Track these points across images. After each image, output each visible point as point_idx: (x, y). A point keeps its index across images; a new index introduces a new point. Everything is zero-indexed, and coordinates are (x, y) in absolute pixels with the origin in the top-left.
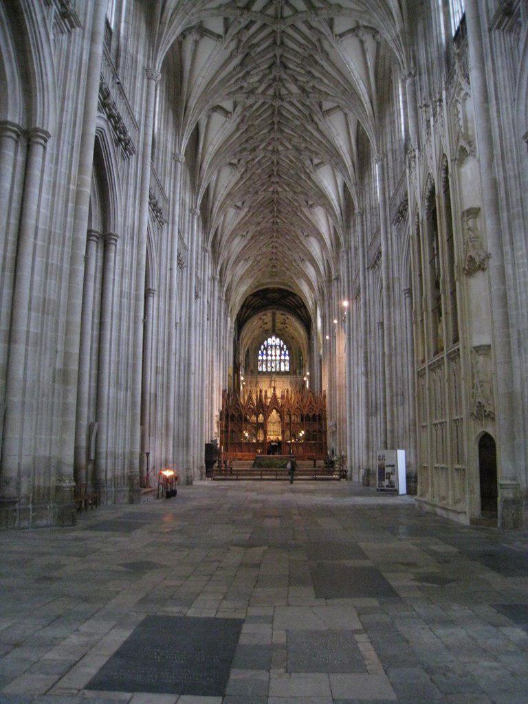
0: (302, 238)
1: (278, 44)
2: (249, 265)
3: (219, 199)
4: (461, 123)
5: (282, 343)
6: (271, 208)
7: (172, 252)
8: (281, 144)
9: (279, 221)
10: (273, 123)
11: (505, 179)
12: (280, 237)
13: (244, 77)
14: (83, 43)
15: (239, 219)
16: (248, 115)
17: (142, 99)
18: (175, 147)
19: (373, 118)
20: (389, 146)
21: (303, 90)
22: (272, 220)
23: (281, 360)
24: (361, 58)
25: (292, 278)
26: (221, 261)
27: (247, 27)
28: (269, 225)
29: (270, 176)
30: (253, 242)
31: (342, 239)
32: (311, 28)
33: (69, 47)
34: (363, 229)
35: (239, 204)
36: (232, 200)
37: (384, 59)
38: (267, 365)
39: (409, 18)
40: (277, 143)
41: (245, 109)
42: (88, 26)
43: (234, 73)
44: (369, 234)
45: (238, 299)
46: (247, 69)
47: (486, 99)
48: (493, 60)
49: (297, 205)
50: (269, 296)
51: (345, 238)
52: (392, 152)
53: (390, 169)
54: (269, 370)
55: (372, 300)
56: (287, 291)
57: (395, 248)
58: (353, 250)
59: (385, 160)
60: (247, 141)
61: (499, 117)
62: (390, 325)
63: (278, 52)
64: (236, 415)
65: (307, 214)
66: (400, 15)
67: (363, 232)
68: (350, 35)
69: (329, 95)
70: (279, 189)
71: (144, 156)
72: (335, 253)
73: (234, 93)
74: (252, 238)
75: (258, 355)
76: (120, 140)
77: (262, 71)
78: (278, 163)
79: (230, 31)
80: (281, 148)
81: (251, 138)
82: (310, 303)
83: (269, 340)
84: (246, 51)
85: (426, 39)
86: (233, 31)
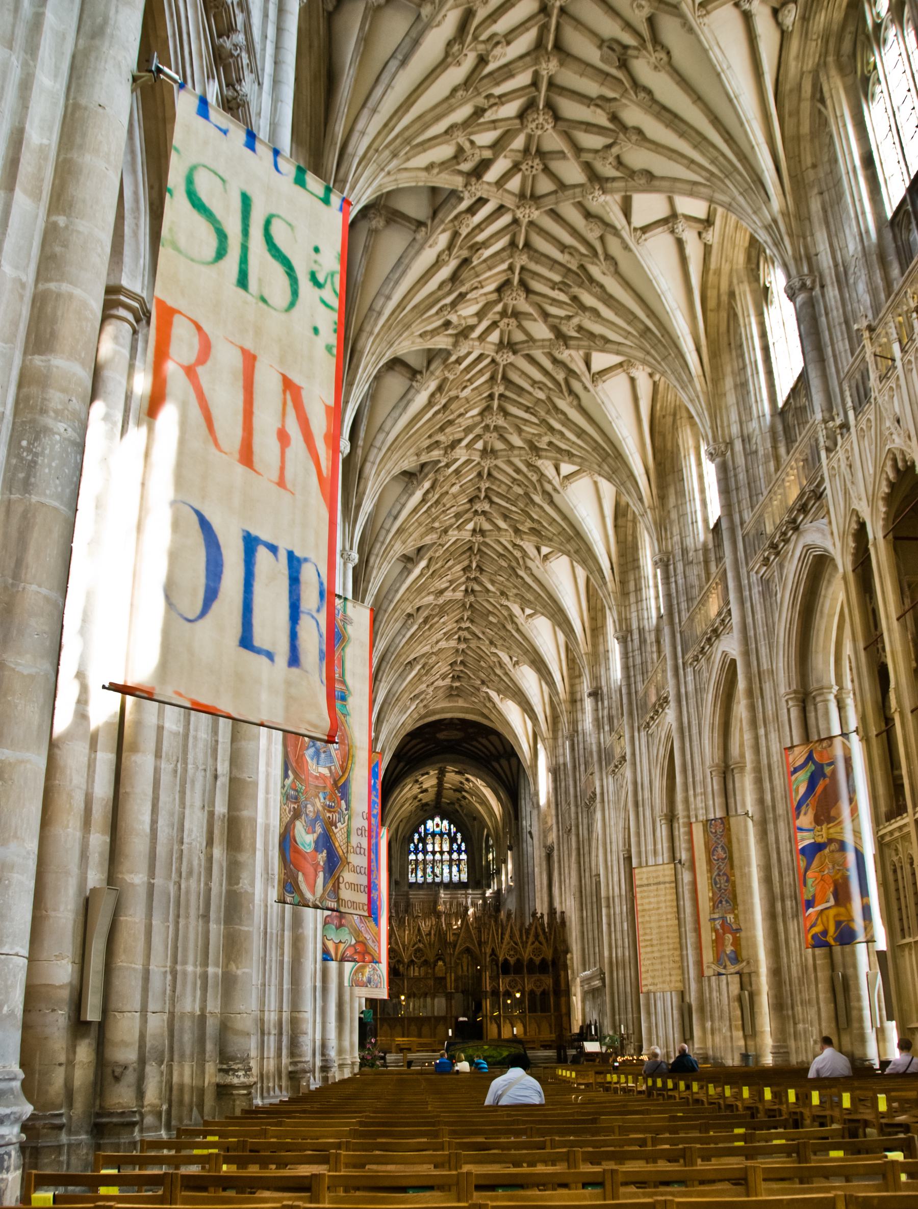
0: (520, 618)
1: (521, 246)
3: (381, 539)
5: (453, 829)
6: (466, 563)
8: (502, 438)
9: (477, 588)
10: (491, 396)
12: (476, 620)
13: (454, 304)
16: (451, 377)
19: (702, 378)
21: (560, 335)
22: (463, 588)
23: (451, 860)
25: (490, 699)
27: (472, 210)
28: (459, 595)
29: (471, 501)
30: (427, 627)
32: (588, 215)
36: (404, 543)
37: (719, 275)
38: (424, 871)
39: (792, 188)
40: (495, 435)
43: (440, 293)
44: (683, 598)
46: (463, 289)
49: (518, 554)
50: (441, 736)
52: (743, 441)
53: (740, 469)
55: (694, 723)
57: (759, 616)
58: (636, 636)
59: (729, 453)
60: (442, 429)
62: (758, 761)
63: (522, 260)
68: (660, 229)
69: (607, 341)
70: (487, 526)
72: (590, 646)
73: (434, 332)
74: (426, 621)
75: (410, 852)
77: (485, 294)
80: (499, 445)
81: (451, 423)
82: (525, 747)
83: (430, 824)
84: (465, 253)
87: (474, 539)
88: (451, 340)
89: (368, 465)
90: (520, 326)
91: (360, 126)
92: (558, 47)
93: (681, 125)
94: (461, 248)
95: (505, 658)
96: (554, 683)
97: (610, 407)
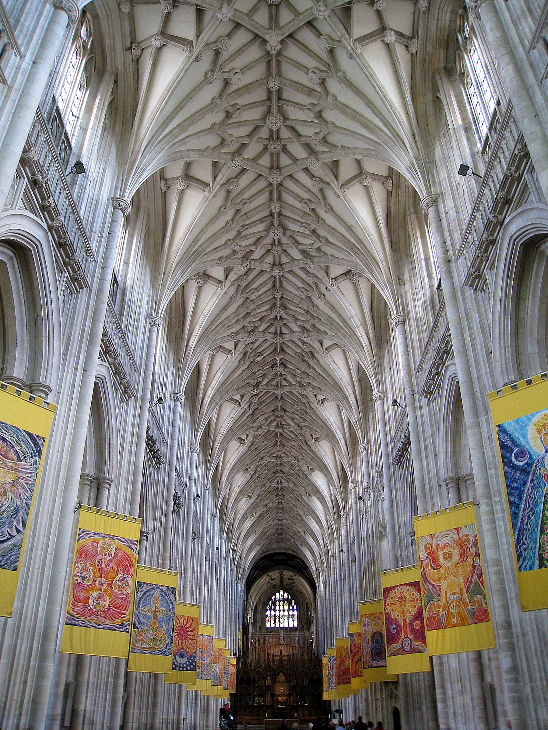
2: (257, 536)
4: (381, 516)
7: (201, 559)
9: (283, 501)
11: (401, 555)
13: (254, 421)
14: (165, 471)
17: (187, 467)
18: (204, 479)
20: (360, 477)
23: (289, 615)
24: (338, 415)
26: (233, 541)
28: (275, 504)
31: (334, 527)
32: (301, 395)
33: (158, 477)
34: (347, 528)
35: (250, 494)
38: (275, 620)
41: (255, 437)
45: (247, 563)
47: (392, 506)
48: (395, 483)
49: (298, 493)
50: (275, 558)
51: (336, 527)
54: (277, 626)
56: (291, 554)
60: (256, 455)
63: (279, 404)
64: (245, 678)
65: (306, 500)
66: (357, 408)
67: (347, 531)
71: (189, 508)
74: (260, 516)
76: (175, 503)
79: (244, 399)
80: (283, 455)
82: (314, 567)
83: (278, 595)
84: (256, 406)
85: (374, 426)
88: (255, 429)
89: (223, 477)
90: (284, 420)
91: (208, 393)
92: (282, 349)
93: (325, 381)
94: (254, 406)
95: (300, 530)
96: (320, 545)
97: (322, 452)
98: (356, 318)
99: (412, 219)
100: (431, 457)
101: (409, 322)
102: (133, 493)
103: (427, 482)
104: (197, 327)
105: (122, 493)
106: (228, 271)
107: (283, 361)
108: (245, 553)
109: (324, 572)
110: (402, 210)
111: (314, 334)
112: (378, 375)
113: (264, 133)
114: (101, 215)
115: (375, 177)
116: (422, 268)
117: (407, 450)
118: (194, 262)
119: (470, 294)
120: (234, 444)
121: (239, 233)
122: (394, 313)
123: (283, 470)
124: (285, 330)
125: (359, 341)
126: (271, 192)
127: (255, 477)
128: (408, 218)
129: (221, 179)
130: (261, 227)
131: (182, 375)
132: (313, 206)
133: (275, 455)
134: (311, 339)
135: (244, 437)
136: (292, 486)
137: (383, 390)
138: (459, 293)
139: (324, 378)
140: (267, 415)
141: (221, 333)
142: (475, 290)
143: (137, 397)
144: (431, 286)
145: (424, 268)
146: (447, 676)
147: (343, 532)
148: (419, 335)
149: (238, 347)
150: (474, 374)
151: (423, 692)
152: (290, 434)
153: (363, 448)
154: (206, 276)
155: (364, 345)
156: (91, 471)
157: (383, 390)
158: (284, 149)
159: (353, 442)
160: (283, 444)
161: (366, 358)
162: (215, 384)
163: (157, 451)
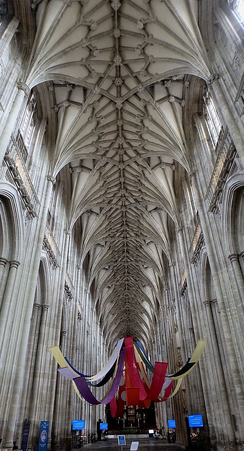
3: (106, 314)
8: (129, 293)
13: (115, 278)
15: (114, 318)
20: (165, 303)
21: (136, 280)
27: (116, 266)
31: (154, 329)
32: (136, 265)
41: (116, 285)
42: (75, 298)
47: (180, 316)
60: (116, 295)
61: (183, 322)
74: (119, 324)
76: (79, 317)
78: (128, 298)
80: (129, 294)
84: (116, 271)
86: (111, 268)
87: (127, 309)
88: (116, 282)
89: (101, 305)
90: (129, 278)
91: (93, 266)
92: (127, 245)
98: (160, 229)
99: (185, 183)
100: (197, 292)
101: (184, 230)
102: (59, 313)
103: (195, 304)
104: (88, 235)
105: (53, 313)
106: (101, 209)
107: (128, 250)
108: (112, 342)
109: (150, 351)
110: (180, 179)
111: (142, 237)
112: (171, 255)
113: (116, 146)
114: (42, 184)
115: (167, 164)
116: (190, 205)
117: (186, 289)
118: (86, 205)
119: (212, 215)
120: (106, 289)
121: (106, 192)
122: (177, 226)
123: (129, 301)
124: (128, 236)
125: (162, 240)
126: (120, 173)
127: (116, 305)
128: (183, 183)
129: (97, 167)
130: (116, 189)
131: (81, 257)
132: (139, 178)
133: (125, 294)
134: (140, 240)
135: (110, 286)
136: (134, 309)
137: (174, 262)
138: (206, 215)
139: (146, 257)
140: (120, 276)
141: (99, 238)
142: (214, 213)
143: (60, 267)
144: (194, 213)
145: (191, 205)
146: (210, 400)
147: (158, 331)
148: (189, 236)
149: (107, 244)
150: (215, 252)
151: (200, 409)
152: (132, 284)
153: (165, 289)
154: (91, 212)
155: (164, 241)
156: (39, 302)
157: (174, 262)
158: (125, 153)
159: (161, 287)
160: (128, 289)
161: (165, 247)
162: (97, 261)
163: (70, 292)
